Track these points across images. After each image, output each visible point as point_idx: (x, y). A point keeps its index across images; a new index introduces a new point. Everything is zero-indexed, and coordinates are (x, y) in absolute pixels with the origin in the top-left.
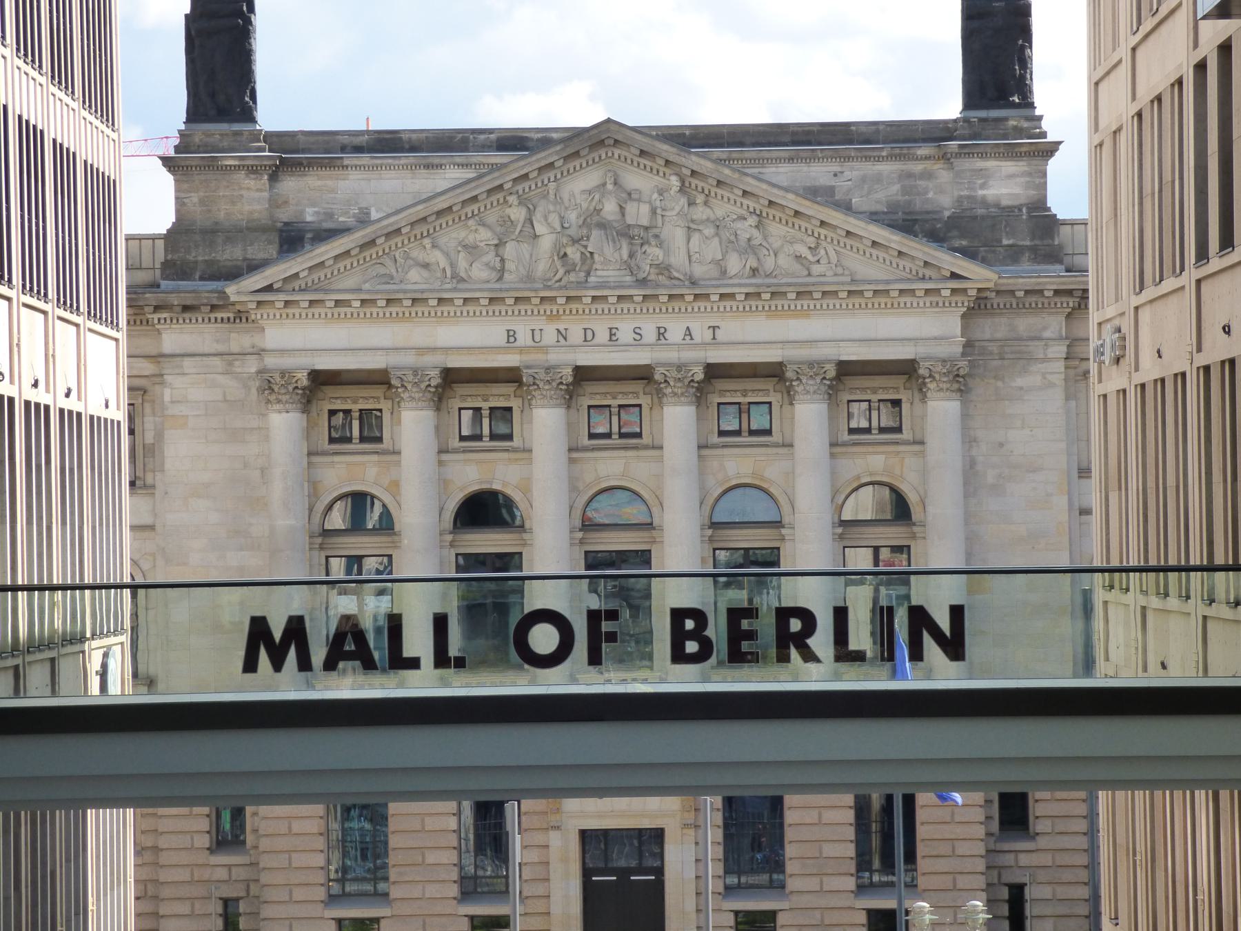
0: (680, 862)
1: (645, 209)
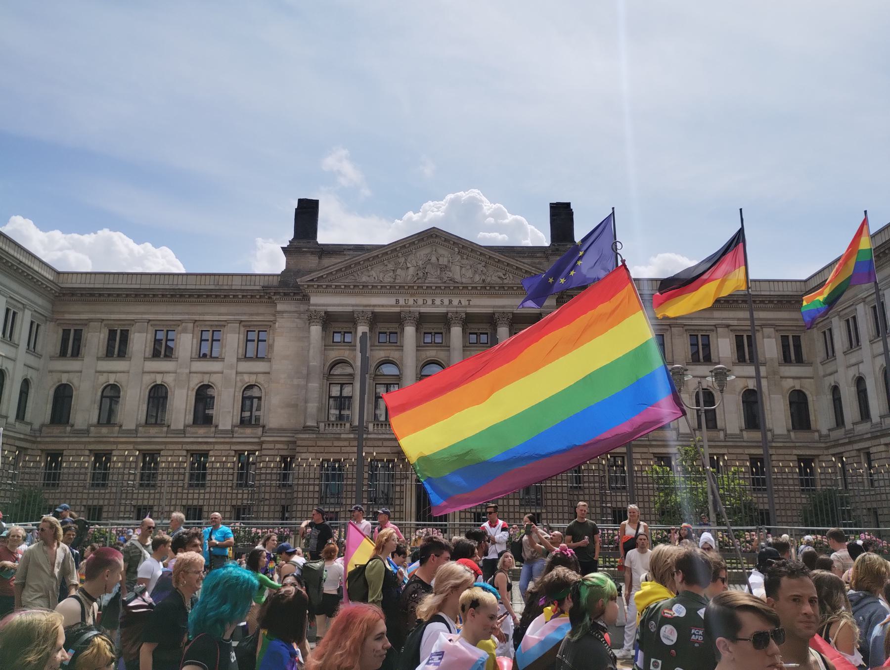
1: (446, 259)
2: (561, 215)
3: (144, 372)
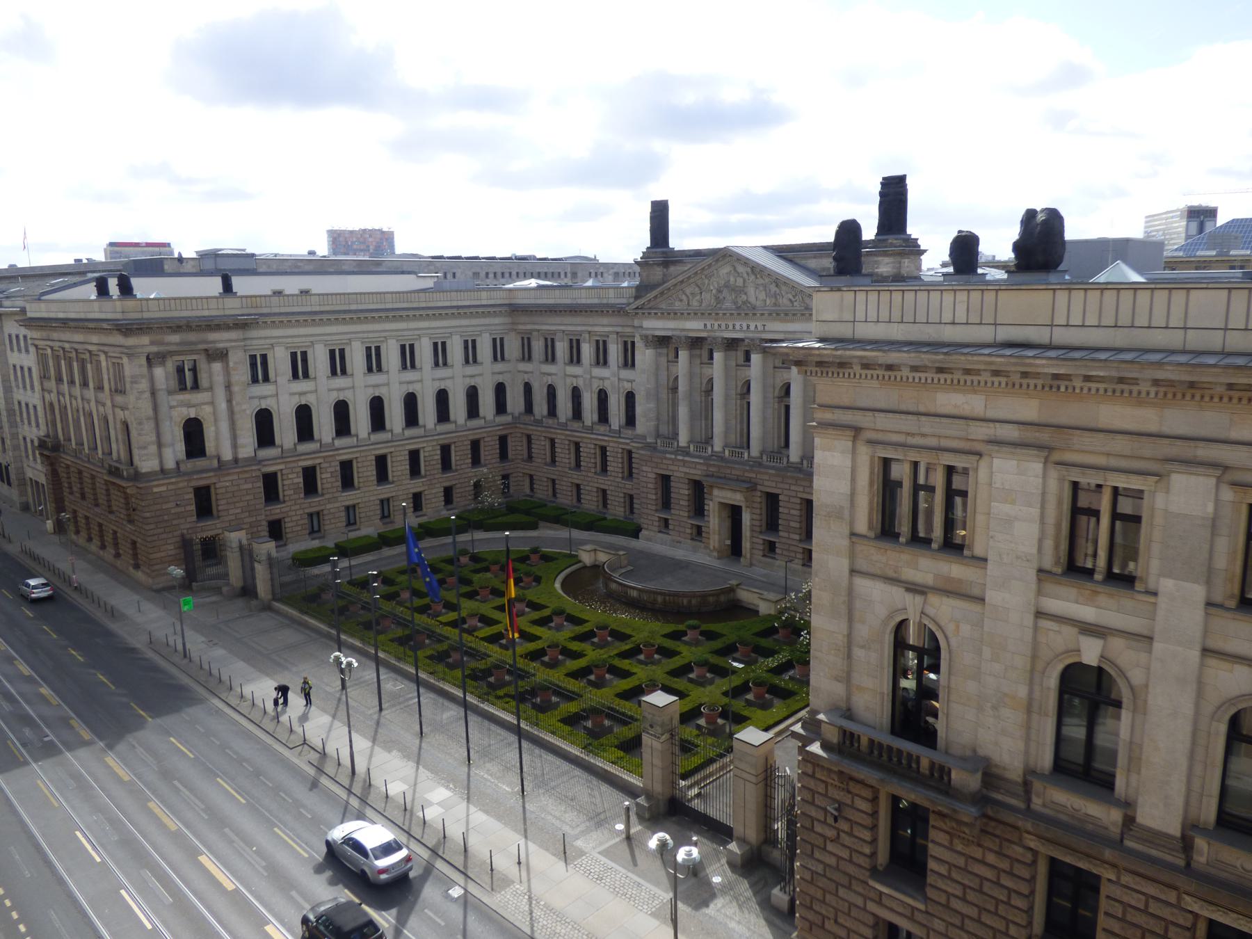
0: (746, 518)
2: (894, 195)
3: (566, 375)
